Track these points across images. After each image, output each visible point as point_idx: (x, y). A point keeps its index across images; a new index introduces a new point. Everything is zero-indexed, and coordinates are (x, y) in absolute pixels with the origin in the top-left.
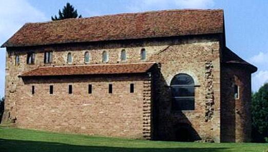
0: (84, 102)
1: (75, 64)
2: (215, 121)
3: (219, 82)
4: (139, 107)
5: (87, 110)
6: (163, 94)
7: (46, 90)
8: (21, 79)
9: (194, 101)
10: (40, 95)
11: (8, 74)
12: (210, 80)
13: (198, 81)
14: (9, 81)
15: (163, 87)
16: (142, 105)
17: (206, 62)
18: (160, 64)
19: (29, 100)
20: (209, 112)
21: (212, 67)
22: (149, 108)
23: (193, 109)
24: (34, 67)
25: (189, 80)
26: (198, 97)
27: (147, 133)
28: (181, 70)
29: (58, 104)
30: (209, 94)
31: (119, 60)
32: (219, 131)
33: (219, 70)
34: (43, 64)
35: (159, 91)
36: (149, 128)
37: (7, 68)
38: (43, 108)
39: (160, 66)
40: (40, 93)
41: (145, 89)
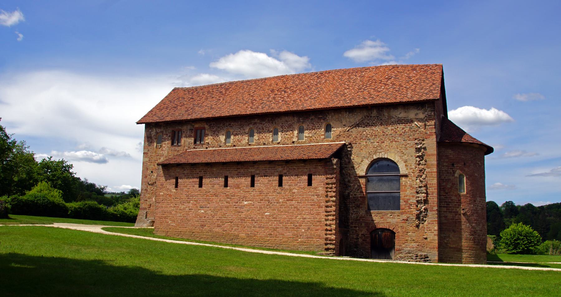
0: (245, 198)
2: (429, 226)
3: (435, 170)
5: (248, 211)
6: (356, 187)
7: (193, 182)
8: (161, 166)
9: (399, 197)
10: (185, 189)
11: (147, 159)
12: (423, 167)
13: (405, 169)
14: (147, 169)
16: (323, 204)
17: (416, 141)
18: (350, 144)
19: (170, 196)
20: (421, 212)
21: (425, 148)
22: (334, 208)
24: (181, 150)
25: (393, 166)
26: (406, 191)
27: (330, 244)
28: (380, 152)
29: (209, 201)
32: (437, 242)
33: (435, 152)
34: (192, 146)
35: (349, 181)
36: (333, 237)
37: (146, 151)
39: (352, 147)
40: (186, 187)
41: (329, 181)
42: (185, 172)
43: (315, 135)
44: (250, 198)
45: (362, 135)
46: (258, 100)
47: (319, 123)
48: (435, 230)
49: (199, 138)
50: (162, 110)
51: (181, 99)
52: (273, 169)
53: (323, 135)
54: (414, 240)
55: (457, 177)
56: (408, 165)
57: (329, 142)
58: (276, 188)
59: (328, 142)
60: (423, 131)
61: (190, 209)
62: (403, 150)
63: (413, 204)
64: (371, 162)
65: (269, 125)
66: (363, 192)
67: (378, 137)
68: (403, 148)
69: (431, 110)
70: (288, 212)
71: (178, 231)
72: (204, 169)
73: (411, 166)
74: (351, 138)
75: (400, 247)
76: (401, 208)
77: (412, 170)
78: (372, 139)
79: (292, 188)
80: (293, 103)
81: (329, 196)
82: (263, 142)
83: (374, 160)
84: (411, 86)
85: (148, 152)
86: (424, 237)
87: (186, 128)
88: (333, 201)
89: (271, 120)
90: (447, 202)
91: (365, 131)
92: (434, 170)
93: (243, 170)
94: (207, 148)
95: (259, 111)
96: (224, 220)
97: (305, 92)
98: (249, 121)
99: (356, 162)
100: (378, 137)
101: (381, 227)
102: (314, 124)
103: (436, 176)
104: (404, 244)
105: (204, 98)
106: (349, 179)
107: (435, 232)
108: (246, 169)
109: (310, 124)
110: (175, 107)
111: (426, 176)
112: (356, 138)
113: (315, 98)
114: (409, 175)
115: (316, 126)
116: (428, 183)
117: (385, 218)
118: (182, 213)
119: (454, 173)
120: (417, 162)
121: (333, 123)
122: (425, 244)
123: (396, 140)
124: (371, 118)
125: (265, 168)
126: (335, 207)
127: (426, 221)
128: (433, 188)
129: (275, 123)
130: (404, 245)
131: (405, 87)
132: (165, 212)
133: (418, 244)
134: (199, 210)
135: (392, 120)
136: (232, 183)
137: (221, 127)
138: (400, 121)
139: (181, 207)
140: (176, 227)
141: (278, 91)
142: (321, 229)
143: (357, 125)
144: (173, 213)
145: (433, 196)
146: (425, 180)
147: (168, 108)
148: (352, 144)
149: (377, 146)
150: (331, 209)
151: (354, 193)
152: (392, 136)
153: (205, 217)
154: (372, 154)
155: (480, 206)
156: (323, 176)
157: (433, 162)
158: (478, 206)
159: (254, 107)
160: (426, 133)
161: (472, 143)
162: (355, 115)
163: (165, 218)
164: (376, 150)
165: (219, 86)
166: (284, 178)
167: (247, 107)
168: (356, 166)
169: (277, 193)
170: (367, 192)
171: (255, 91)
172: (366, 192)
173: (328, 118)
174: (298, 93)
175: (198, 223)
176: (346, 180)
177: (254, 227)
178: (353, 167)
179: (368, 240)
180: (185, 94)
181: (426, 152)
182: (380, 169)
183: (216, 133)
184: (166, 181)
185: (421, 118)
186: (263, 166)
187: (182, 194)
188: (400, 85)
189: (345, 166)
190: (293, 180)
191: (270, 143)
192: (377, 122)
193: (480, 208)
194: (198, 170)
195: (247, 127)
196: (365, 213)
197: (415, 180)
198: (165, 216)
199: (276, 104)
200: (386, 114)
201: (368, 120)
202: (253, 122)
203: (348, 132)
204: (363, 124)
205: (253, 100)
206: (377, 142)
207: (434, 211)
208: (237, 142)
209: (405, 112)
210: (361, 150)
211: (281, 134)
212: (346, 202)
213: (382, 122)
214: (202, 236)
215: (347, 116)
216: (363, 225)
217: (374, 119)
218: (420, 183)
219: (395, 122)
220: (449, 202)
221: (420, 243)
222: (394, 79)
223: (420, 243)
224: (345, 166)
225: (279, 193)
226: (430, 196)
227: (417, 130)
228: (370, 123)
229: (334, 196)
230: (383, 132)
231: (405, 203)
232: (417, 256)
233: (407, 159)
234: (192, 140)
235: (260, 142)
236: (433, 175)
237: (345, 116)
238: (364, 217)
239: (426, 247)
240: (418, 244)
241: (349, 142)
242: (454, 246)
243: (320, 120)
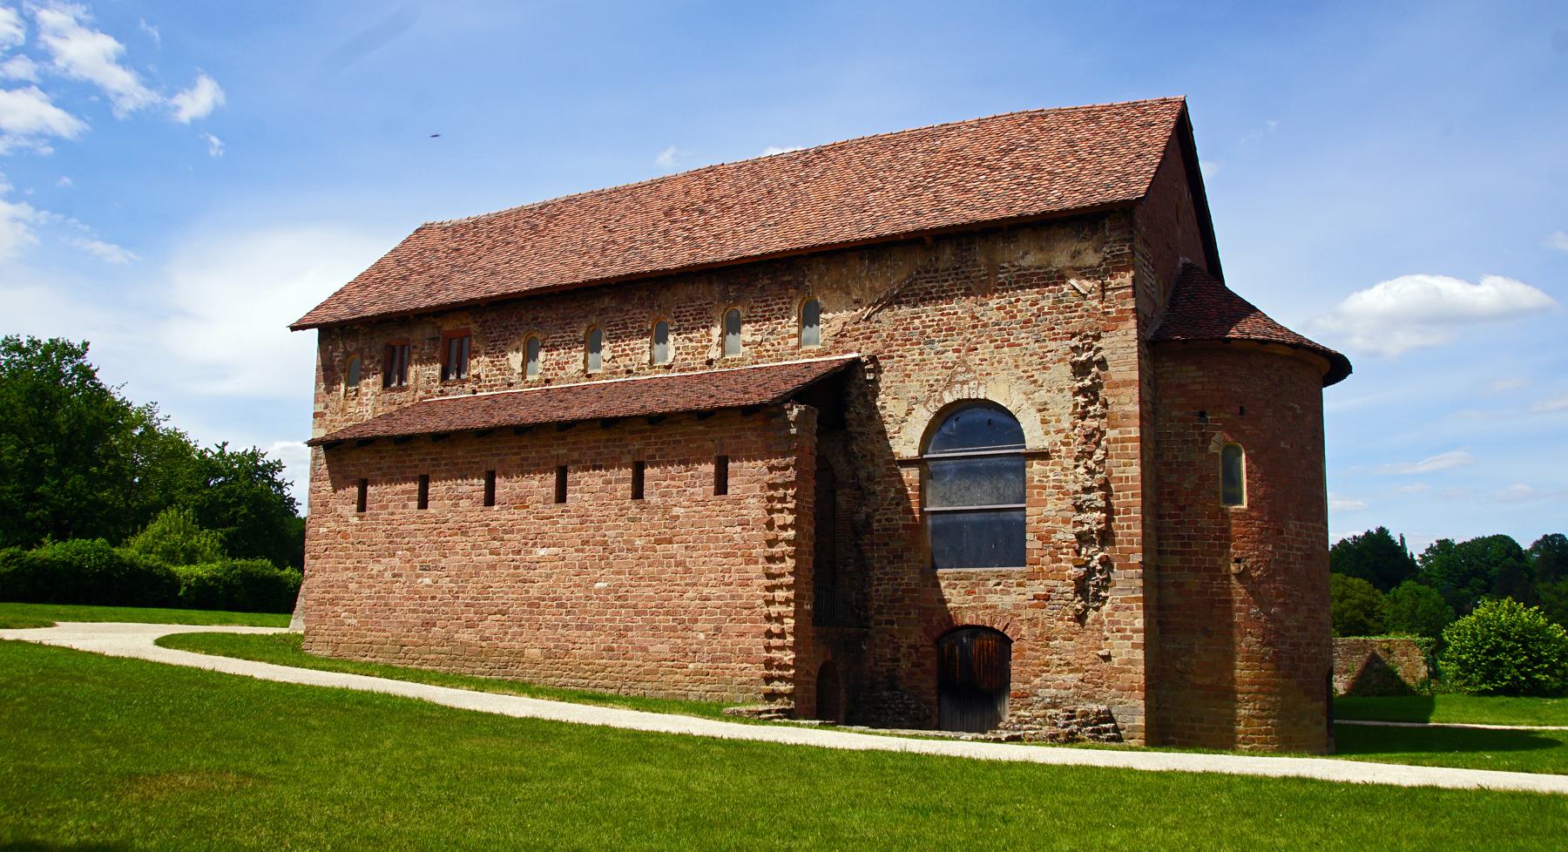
0: (539, 539)
1: (548, 381)
2: (1117, 616)
3: (1135, 432)
4: (750, 560)
5: (549, 576)
7: (404, 492)
8: (321, 447)
9: (1024, 524)
10: (384, 515)
12: (1095, 424)
16: (760, 551)
17: (1075, 342)
18: (873, 359)
19: (345, 536)
20: (1091, 572)
22: (790, 564)
25: (999, 423)
26: (1043, 503)
27: (781, 679)
28: (963, 383)
29: (445, 550)
30: (1088, 490)
32: (1141, 668)
34: (436, 387)
35: (870, 478)
36: (788, 657)
39: (878, 370)
40: (385, 507)
41: (777, 477)
42: (385, 463)
45: (908, 329)
46: (621, 240)
48: (1135, 631)
49: (453, 366)
50: (368, 286)
51: (427, 253)
52: (618, 446)
53: (795, 336)
54: (1068, 664)
55: (1217, 454)
58: (626, 505)
59: (809, 357)
60: (1095, 308)
61: (394, 576)
62: (1034, 372)
63: (1066, 547)
64: (939, 414)
65: (641, 313)
66: (911, 511)
67: (958, 334)
68: (1035, 367)
69: (1122, 236)
70: (660, 580)
71: (363, 641)
72: (431, 453)
74: (875, 342)
75: (1028, 686)
76: (1029, 558)
77: (1061, 436)
78: (939, 342)
79: (670, 501)
80: (710, 244)
81: (776, 524)
82: (625, 366)
83: (947, 407)
84: (1068, 167)
85: (325, 411)
86: (1100, 653)
87: (419, 335)
88: (789, 540)
90: (1183, 537)
91: (920, 317)
92: (1130, 432)
93: (537, 452)
94: (474, 392)
95: (615, 270)
96: (484, 605)
97: (754, 209)
99: (890, 416)
100: (958, 334)
101: (967, 621)
103: (1137, 452)
104: (1037, 676)
105: (486, 246)
107: (1135, 635)
110: (404, 278)
111: (1106, 455)
112: (892, 339)
113: (776, 224)
114: (1053, 451)
115: (773, 310)
116: (1114, 475)
117: (980, 593)
118: (375, 586)
119: (1206, 440)
120: (1079, 409)
121: (824, 297)
122: (1105, 676)
123: (1012, 341)
125: (595, 441)
126: (794, 561)
127: (1108, 601)
128: (1130, 493)
129: (659, 306)
130: (1037, 681)
131: (1049, 173)
132: (332, 586)
133: (1080, 675)
134: (418, 576)
135: (1000, 278)
136: (505, 493)
137: (512, 326)
138: (1025, 280)
140: (359, 629)
141: (683, 211)
142: (755, 630)
143: (893, 301)
144: (353, 586)
145: (1129, 519)
146: (1104, 467)
147: (386, 280)
148: (880, 358)
149: (955, 363)
150: (783, 568)
151: (886, 514)
152: (1000, 330)
153: (433, 598)
154: (940, 389)
155: (1298, 549)
156: (760, 463)
157: (1127, 408)
159: (601, 263)
160: (1104, 313)
161: (1262, 342)
162: (887, 267)
163: (333, 602)
164: (952, 376)
165: (536, 211)
166: (648, 472)
167: (584, 264)
168: (890, 428)
169: (629, 519)
170: (925, 509)
171: (624, 216)
172: (921, 511)
174: (736, 214)
175: (415, 615)
176: (862, 474)
177: (564, 627)
178: (883, 432)
179: (930, 664)
180: (443, 240)
181: (1105, 375)
182: (968, 436)
183: (498, 348)
184: (335, 491)
185: (1091, 267)
187: (375, 530)
188: (1037, 168)
189: (860, 429)
190: (673, 479)
191: (644, 369)
192: (955, 285)
193: (1299, 553)
195: (581, 322)
196: (918, 576)
197: (1072, 467)
198: (331, 596)
199: (666, 248)
200: (982, 259)
201: (927, 282)
202: (597, 305)
203: (868, 323)
204: (912, 295)
206: (956, 351)
207: (1132, 567)
208: (554, 369)
209: (1041, 250)
211: (675, 339)
212: (860, 542)
213: (971, 285)
214: (426, 656)
216: (912, 616)
217: (946, 277)
218: (1087, 477)
219: (1010, 283)
220: (1189, 537)
221: (1087, 671)
222: (1022, 151)
223: (1087, 671)
224: (860, 429)
225: (633, 520)
226: (1121, 520)
227: (1077, 306)
228: (933, 291)
229: (791, 526)
230: (973, 317)
231: (1039, 544)
232: (1074, 717)
233: (1046, 399)
234: (435, 370)
235: (618, 367)
236: (1127, 448)
239: (1108, 687)
240: (1080, 675)
241: (870, 352)
242: (1208, 681)
243: (787, 290)
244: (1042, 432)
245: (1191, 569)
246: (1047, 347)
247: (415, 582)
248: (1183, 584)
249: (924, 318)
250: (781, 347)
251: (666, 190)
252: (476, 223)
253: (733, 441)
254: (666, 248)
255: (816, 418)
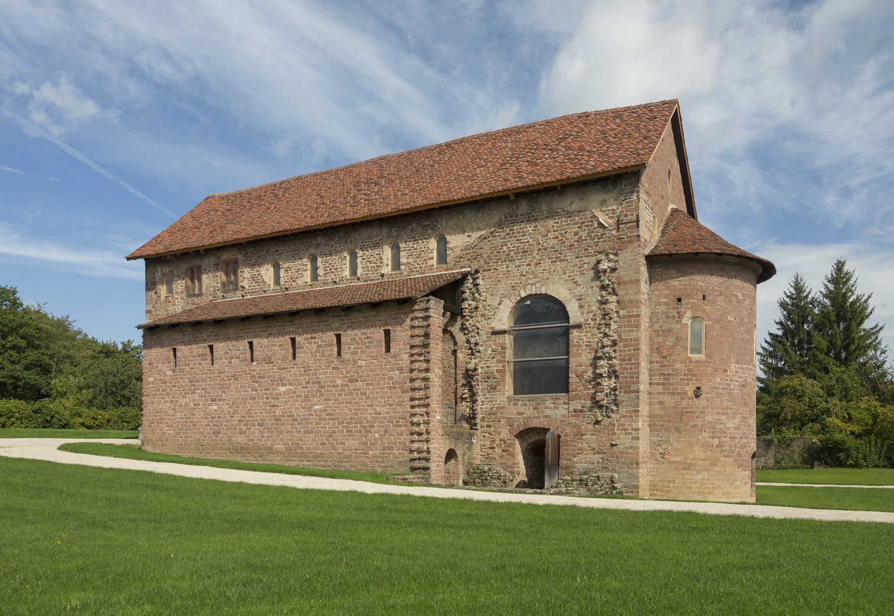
1: (287, 289)
6: (489, 352)
9: (568, 368)
10: (187, 369)
15: (487, 333)
19: (164, 383)
23: (567, 390)
26: (580, 355)
28: (534, 284)
29: (224, 388)
31: (387, 270)
34: (219, 294)
37: (150, 307)
38: (194, 401)
40: (188, 365)
43: (418, 260)
44: (289, 379)
45: (499, 252)
47: (425, 235)
51: (212, 212)
52: (325, 325)
55: (687, 324)
56: (583, 304)
57: (442, 271)
61: (195, 405)
65: (340, 246)
72: (214, 332)
73: (589, 306)
76: (571, 388)
77: (591, 315)
80: (380, 203)
82: (332, 279)
89: (344, 237)
90: (665, 375)
91: (507, 245)
98: (307, 242)
99: (489, 305)
102: (416, 238)
105: (247, 208)
106: (478, 337)
107: (633, 432)
108: (280, 328)
109: (408, 240)
110: (197, 228)
123: (562, 258)
124: (516, 218)
125: (311, 323)
128: (632, 348)
129: (351, 242)
136: (260, 355)
139: (182, 402)
141: (365, 183)
145: (632, 364)
149: (527, 272)
158: (732, 380)
162: (487, 214)
173: (440, 225)
180: (221, 204)
186: (309, 320)
190: (358, 343)
191: (343, 280)
194: (205, 334)
199: (354, 206)
202: (314, 242)
205: (320, 204)
206: (528, 265)
207: (633, 392)
210: (498, 283)
211: (361, 262)
215: (474, 218)
231: (577, 380)
237: (469, 217)
238: (503, 408)
242: (678, 459)
243: (427, 230)
244: (580, 313)
245: (669, 394)
246: (583, 261)
247: (208, 408)
248: (664, 402)
249: (509, 245)
250: (424, 265)
251: (356, 171)
252: (241, 194)
253: (393, 321)
254: (354, 206)
255: (442, 306)
